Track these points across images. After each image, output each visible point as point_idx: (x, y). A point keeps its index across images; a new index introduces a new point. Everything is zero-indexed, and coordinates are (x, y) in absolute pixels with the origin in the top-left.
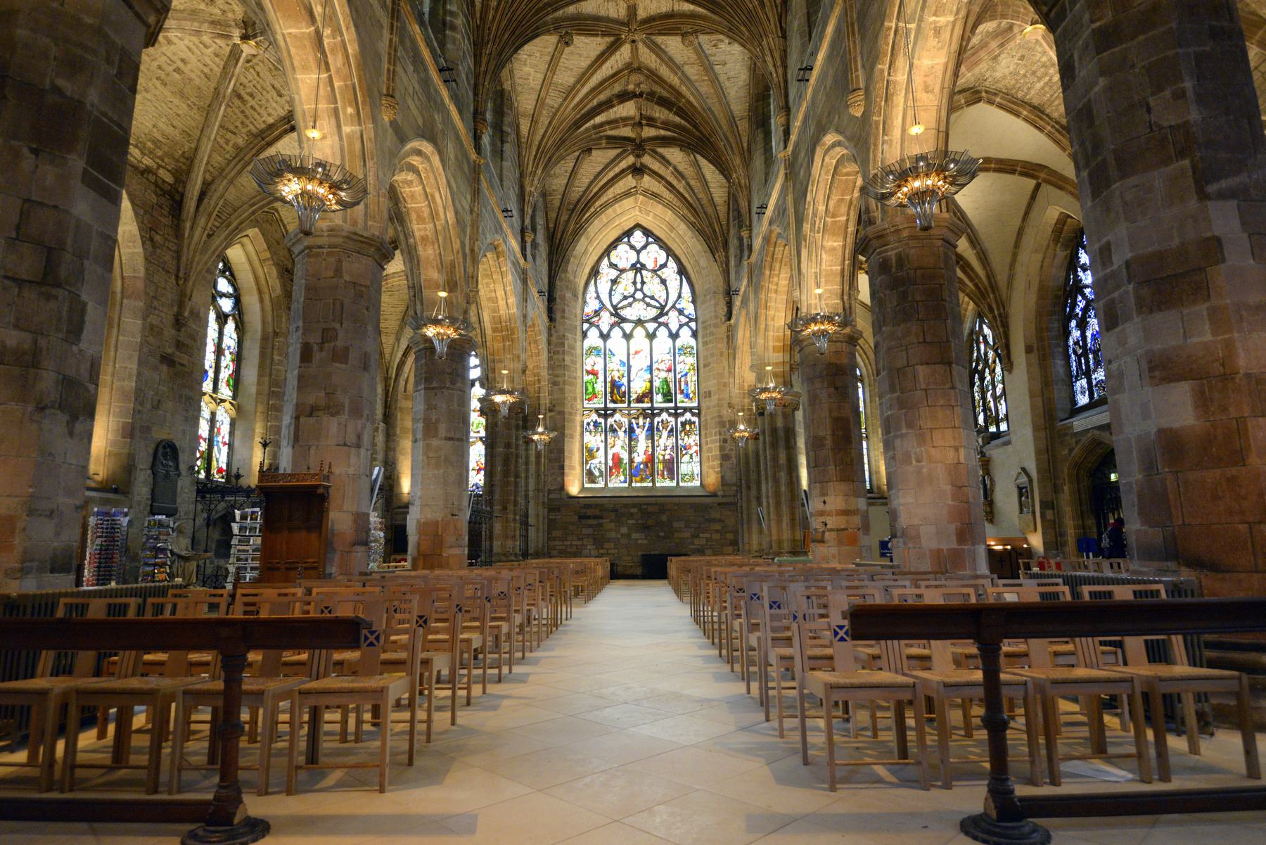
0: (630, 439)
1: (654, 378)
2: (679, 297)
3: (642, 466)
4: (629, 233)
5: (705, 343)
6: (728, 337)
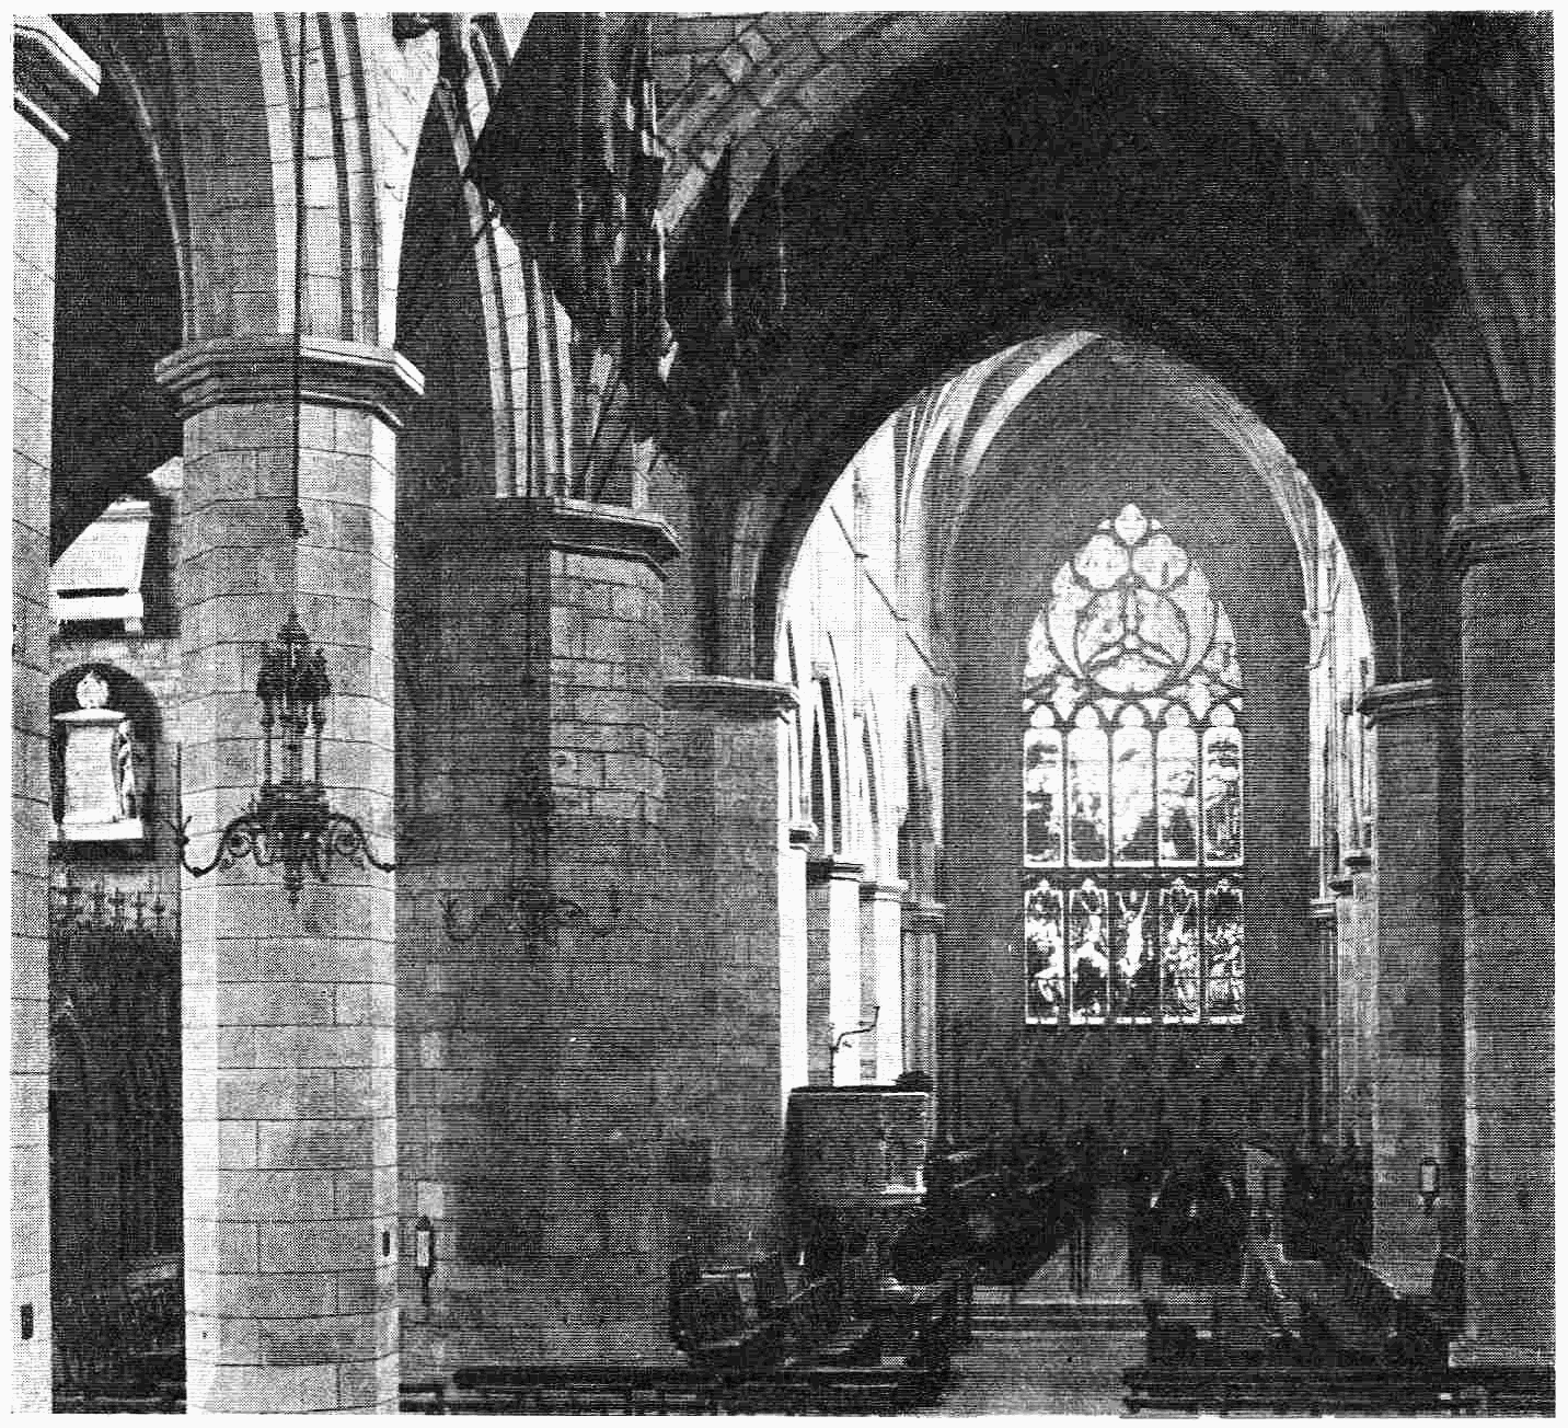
1: (1160, 810)
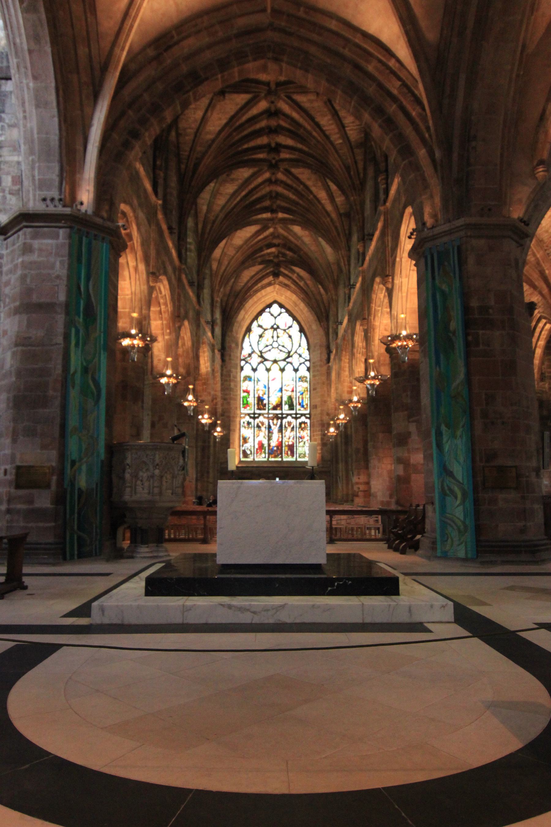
0: (269, 432)
2: (300, 346)
3: (275, 448)
4: (270, 306)
5: (314, 376)
6: (327, 373)
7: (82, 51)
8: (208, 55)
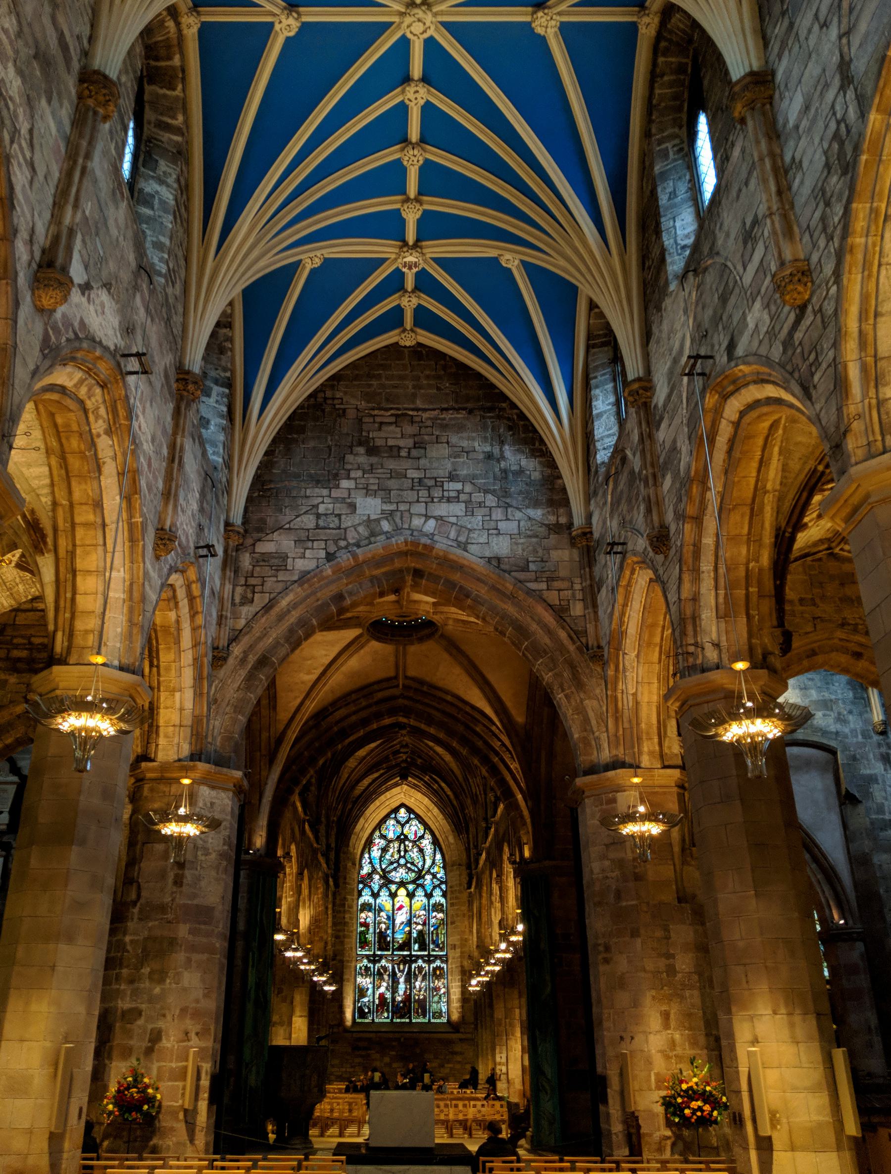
0: (393, 982)
2: (433, 863)
4: (396, 810)
7: (265, 735)
8: (354, 718)
